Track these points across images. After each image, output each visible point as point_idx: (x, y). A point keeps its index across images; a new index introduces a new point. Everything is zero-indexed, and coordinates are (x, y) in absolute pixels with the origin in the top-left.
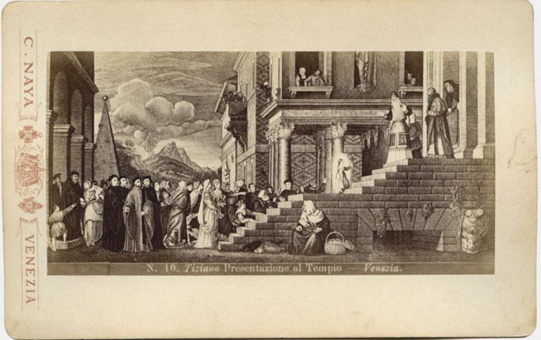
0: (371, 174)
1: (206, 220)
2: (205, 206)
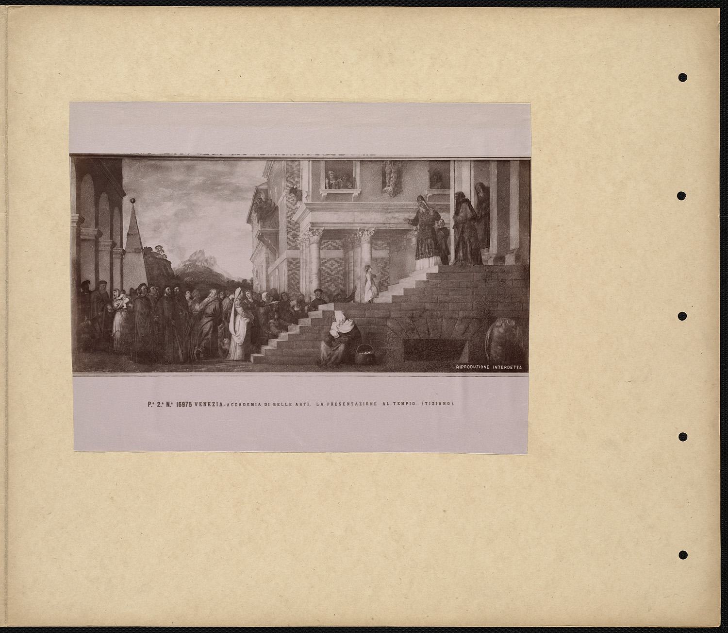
1: (237, 329)
2: (236, 314)
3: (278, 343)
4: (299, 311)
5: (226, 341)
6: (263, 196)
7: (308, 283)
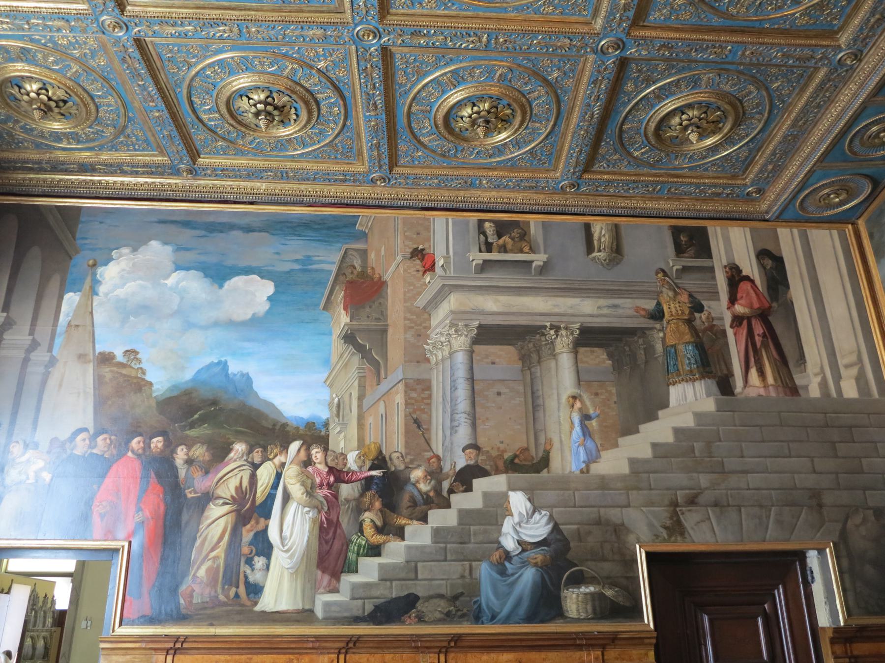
0: (637, 431)
1: (287, 532)
2: (287, 498)
3: (381, 567)
4: (429, 491)
5: (259, 562)
6: (357, 263)
7: (448, 432)
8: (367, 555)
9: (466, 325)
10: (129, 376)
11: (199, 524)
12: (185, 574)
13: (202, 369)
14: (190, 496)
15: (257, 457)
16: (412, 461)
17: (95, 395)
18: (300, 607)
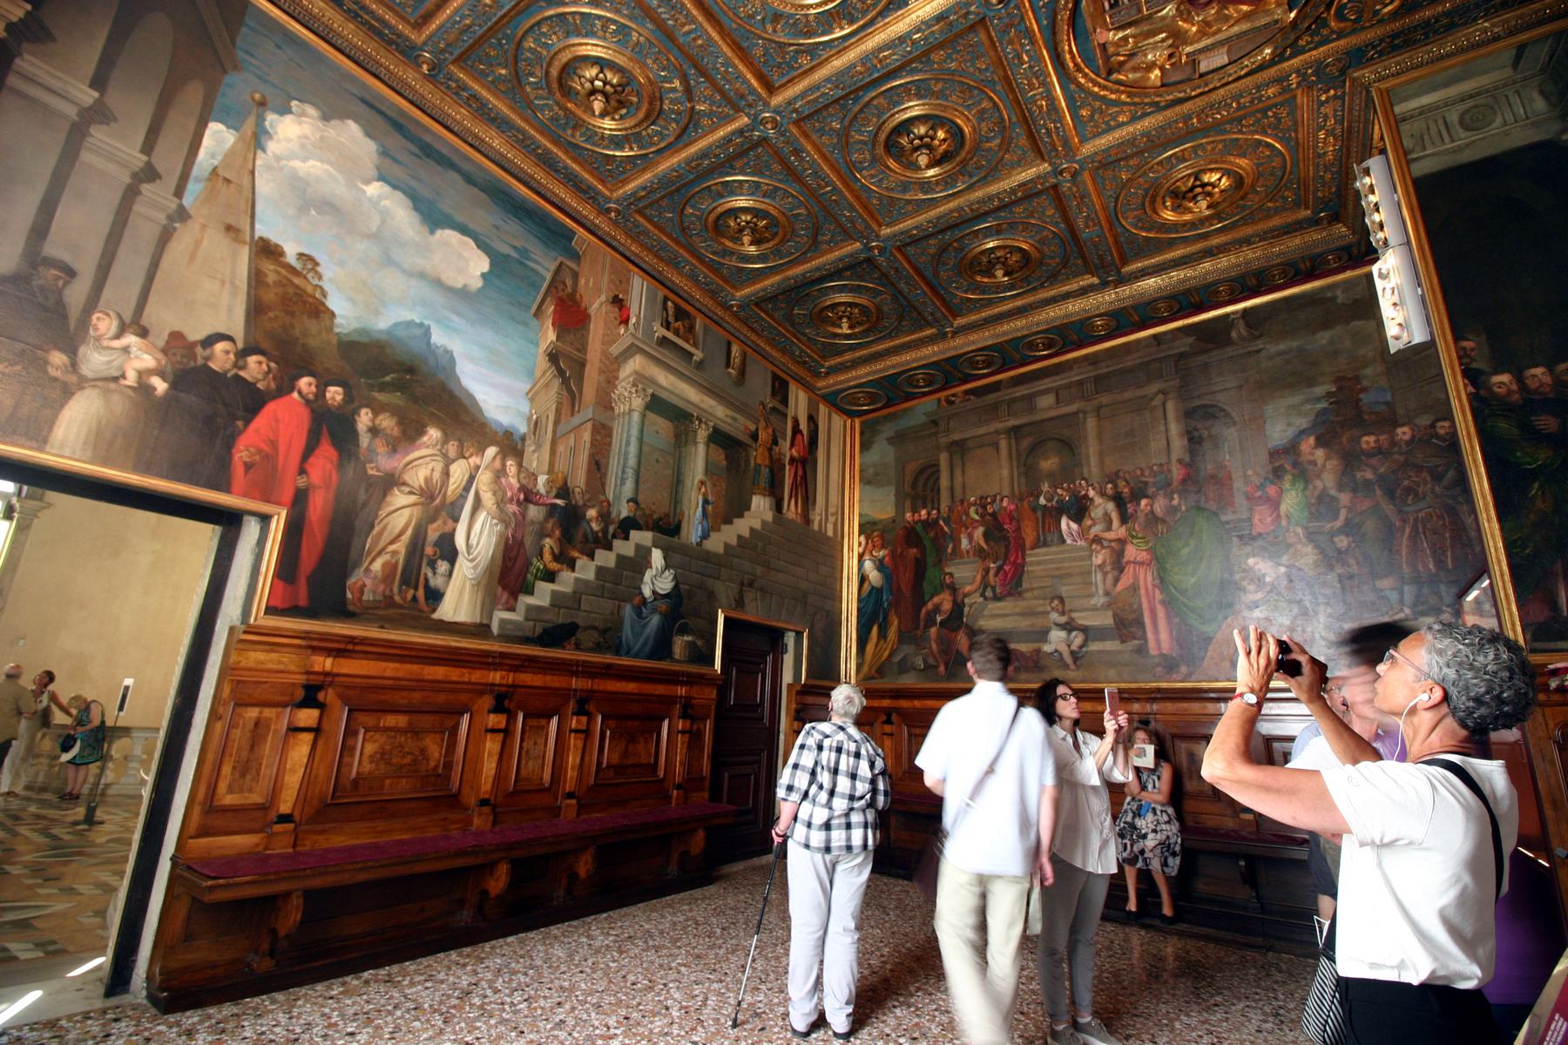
0: (731, 523)
1: (473, 540)
3: (554, 593)
5: (443, 566)
6: (569, 282)
8: (543, 580)
9: (644, 390)
10: (304, 291)
11: (379, 509)
12: (357, 564)
13: (401, 323)
14: (370, 472)
15: (452, 449)
16: (589, 500)
17: (248, 294)
18: (478, 621)
